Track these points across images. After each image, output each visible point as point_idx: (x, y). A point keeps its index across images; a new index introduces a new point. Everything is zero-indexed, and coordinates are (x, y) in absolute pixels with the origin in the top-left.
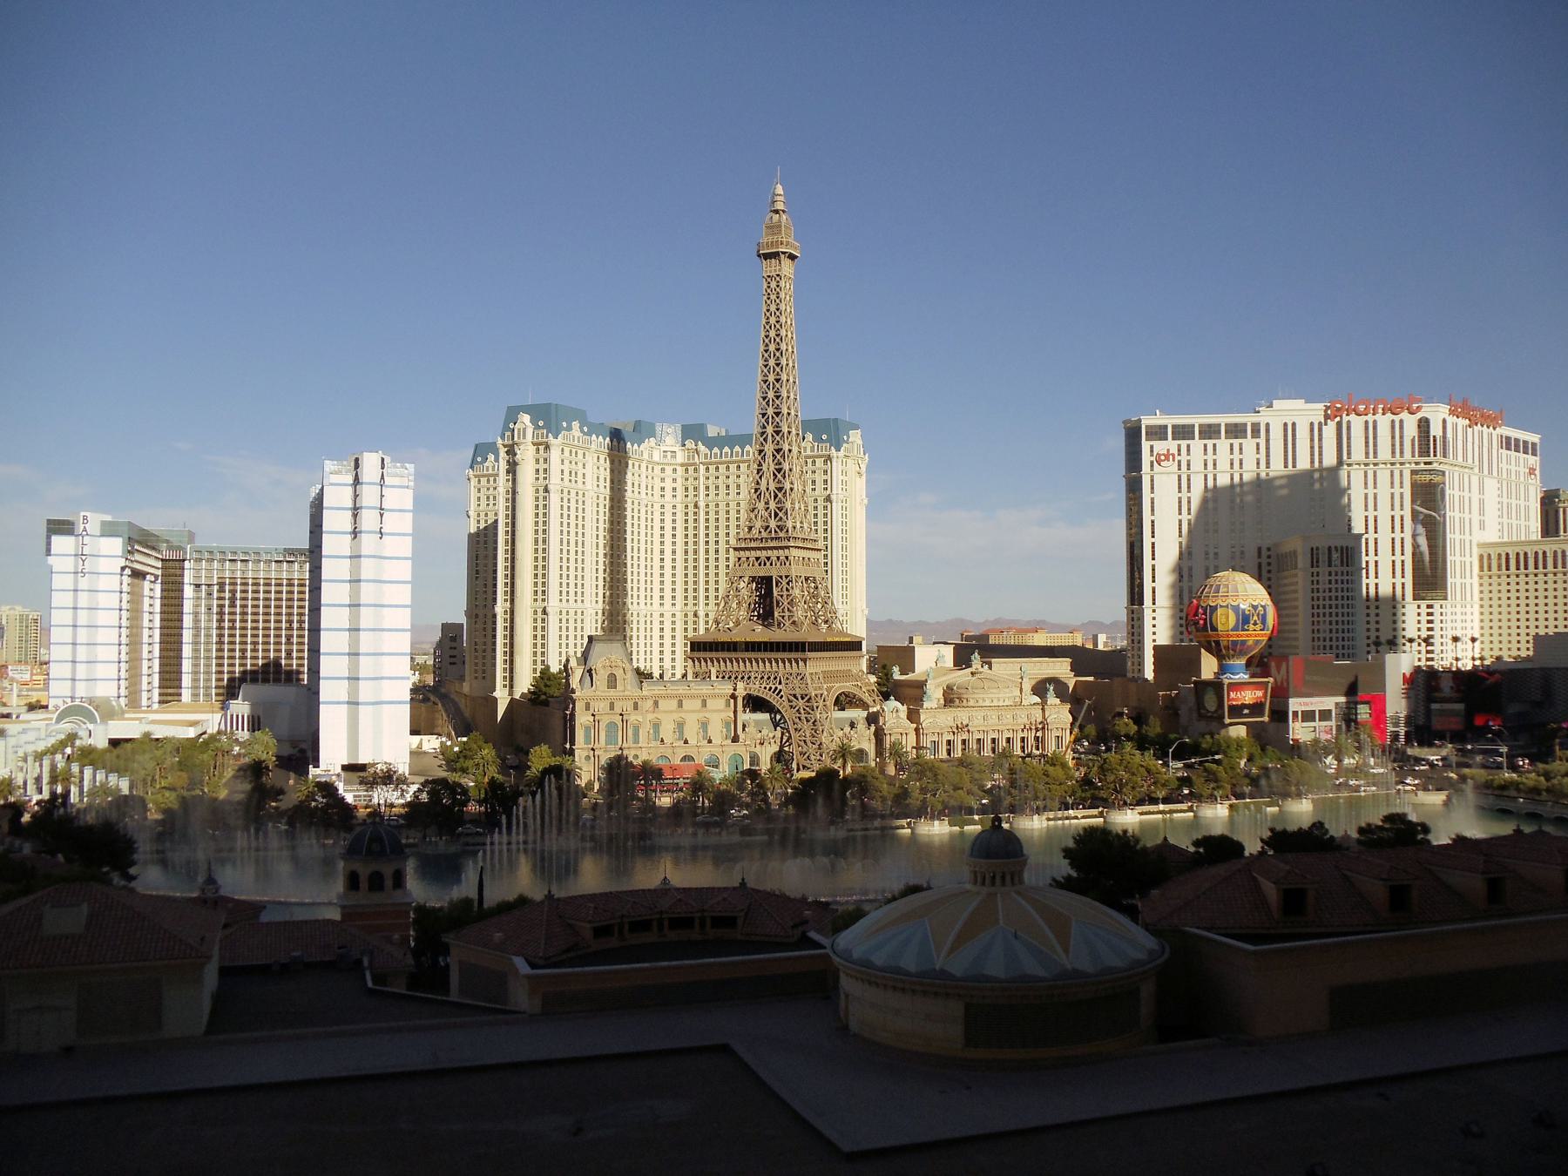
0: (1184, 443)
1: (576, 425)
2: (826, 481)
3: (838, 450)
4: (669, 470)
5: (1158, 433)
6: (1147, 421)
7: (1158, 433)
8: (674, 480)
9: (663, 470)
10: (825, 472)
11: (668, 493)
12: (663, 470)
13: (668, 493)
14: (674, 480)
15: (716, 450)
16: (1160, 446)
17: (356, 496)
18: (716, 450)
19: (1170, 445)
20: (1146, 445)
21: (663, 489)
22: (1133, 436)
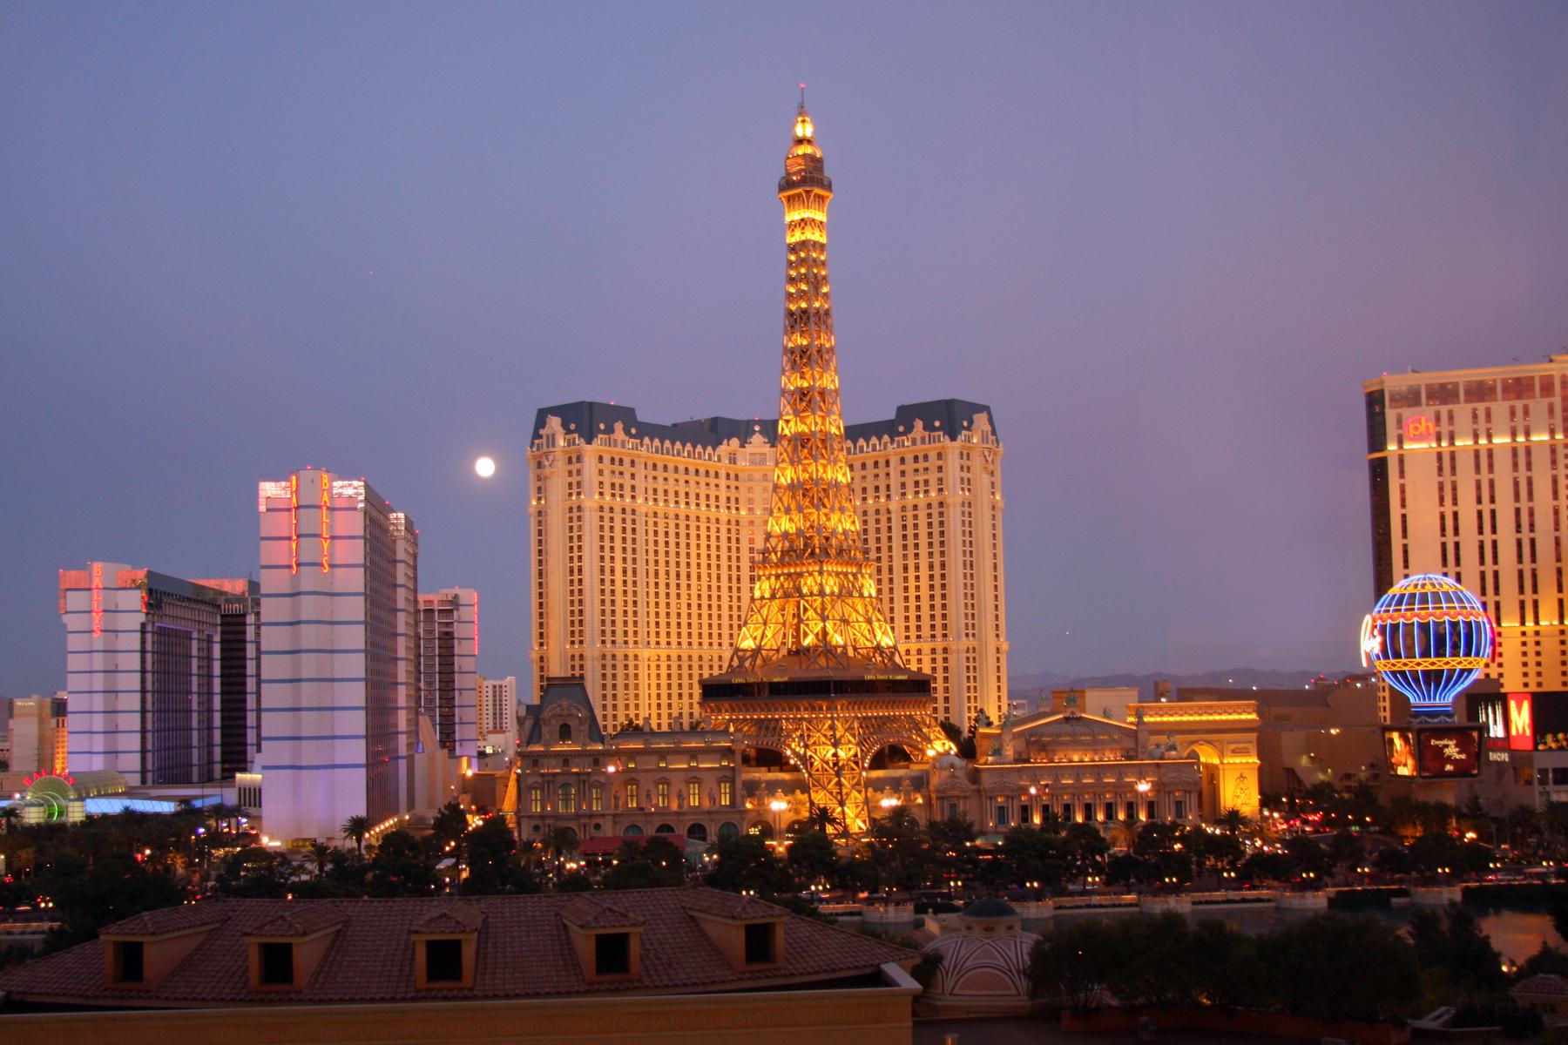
0: (1444, 409)
1: (619, 426)
2: (940, 480)
3: (953, 439)
10: (940, 469)
20: (1391, 415)
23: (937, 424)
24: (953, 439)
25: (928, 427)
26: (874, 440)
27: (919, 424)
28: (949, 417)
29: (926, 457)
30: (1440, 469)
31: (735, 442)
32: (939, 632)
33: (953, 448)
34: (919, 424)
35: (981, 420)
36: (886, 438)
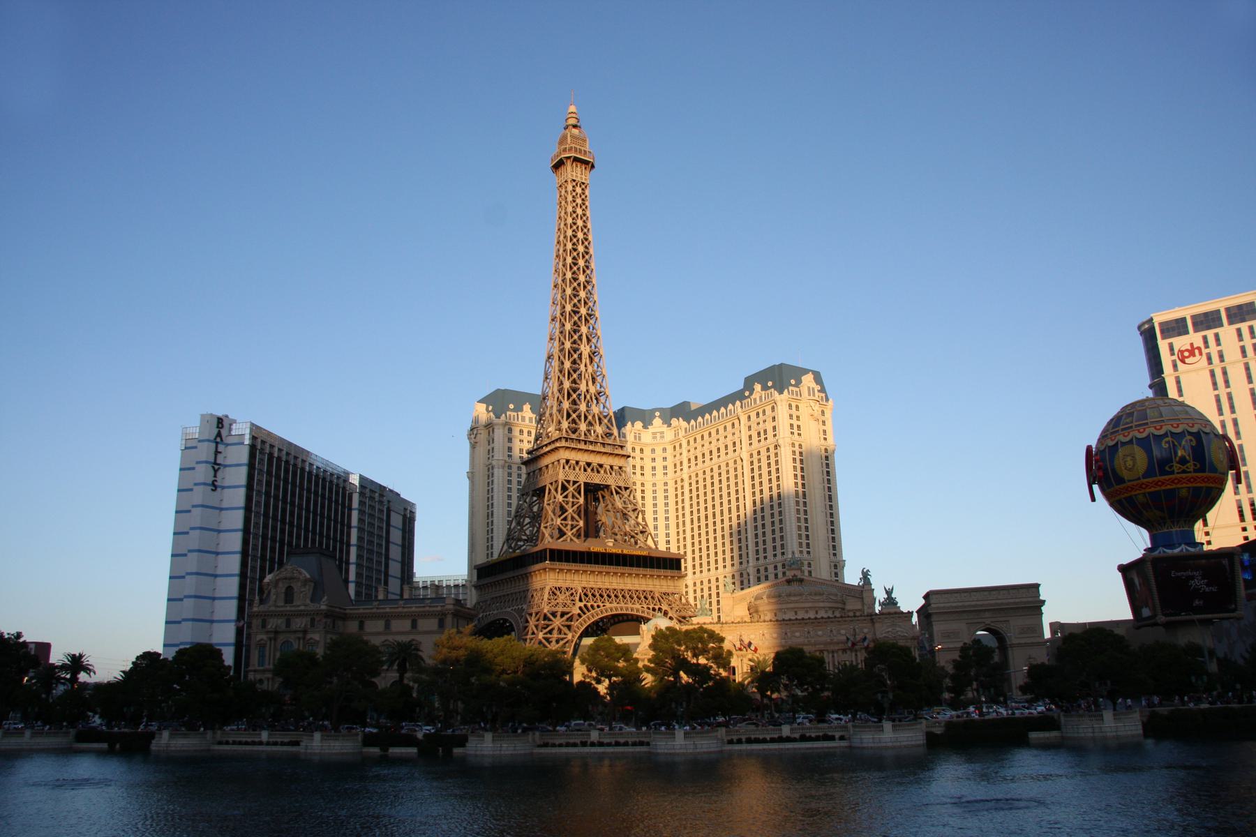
0: (1210, 334)
3: (781, 392)
4: (659, 450)
5: (1177, 328)
6: (1159, 318)
7: (1177, 328)
8: (665, 459)
9: (653, 451)
11: (660, 471)
12: (653, 451)
13: (660, 471)
14: (665, 459)
15: (693, 422)
16: (1181, 342)
17: (217, 452)
18: (693, 422)
19: (1194, 338)
20: (1163, 345)
21: (654, 468)
22: (1149, 335)
23: (770, 384)
24: (781, 392)
25: (765, 388)
26: (730, 406)
27: (758, 387)
28: (779, 377)
29: (764, 412)
30: (1215, 384)
31: (639, 425)
32: (779, 551)
33: (782, 399)
34: (758, 387)
35: (808, 380)
36: (738, 403)
